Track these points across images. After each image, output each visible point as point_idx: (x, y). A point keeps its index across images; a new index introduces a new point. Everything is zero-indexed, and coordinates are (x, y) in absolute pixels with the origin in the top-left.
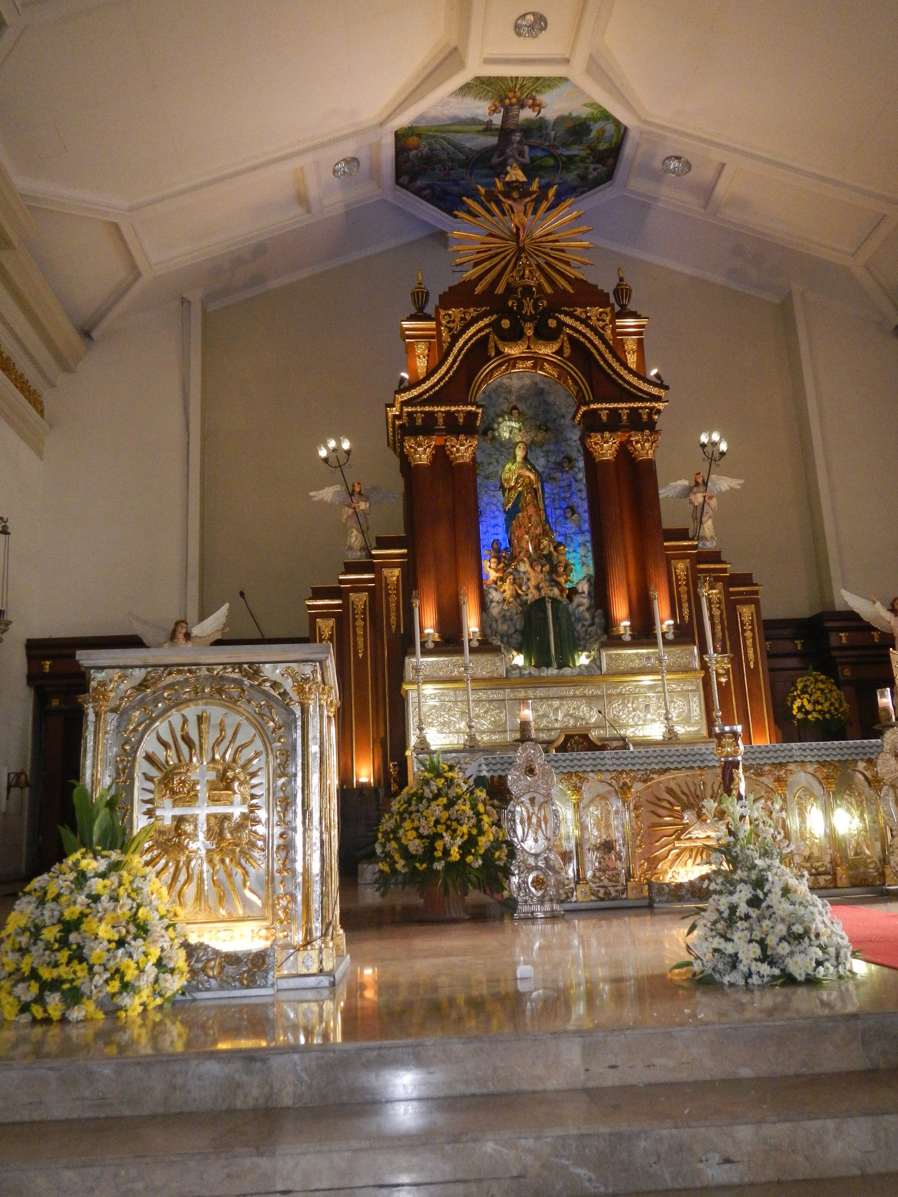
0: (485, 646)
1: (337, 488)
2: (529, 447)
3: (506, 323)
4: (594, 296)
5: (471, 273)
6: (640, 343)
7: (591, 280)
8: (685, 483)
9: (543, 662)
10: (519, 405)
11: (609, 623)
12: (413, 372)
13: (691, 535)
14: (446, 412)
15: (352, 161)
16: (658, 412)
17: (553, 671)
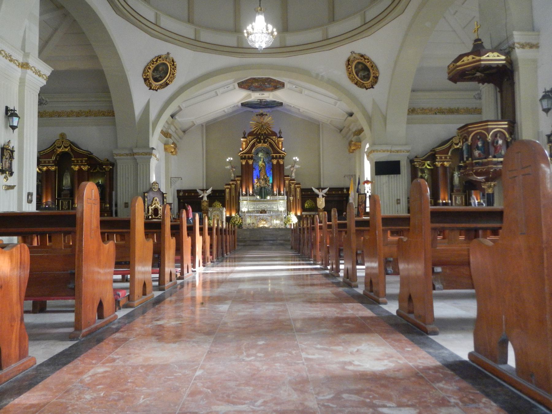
0: (253, 195)
1: (230, 166)
2: (263, 158)
3: (258, 140)
4: (274, 134)
5: (253, 130)
6: (282, 143)
7: (274, 131)
8: (290, 166)
9: (262, 198)
10: (264, 149)
11: (273, 192)
12: (243, 148)
13: (290, 176)
14: (248, 156)
15: (234, 106)
16: (285, 155)
17: (263, 199)
